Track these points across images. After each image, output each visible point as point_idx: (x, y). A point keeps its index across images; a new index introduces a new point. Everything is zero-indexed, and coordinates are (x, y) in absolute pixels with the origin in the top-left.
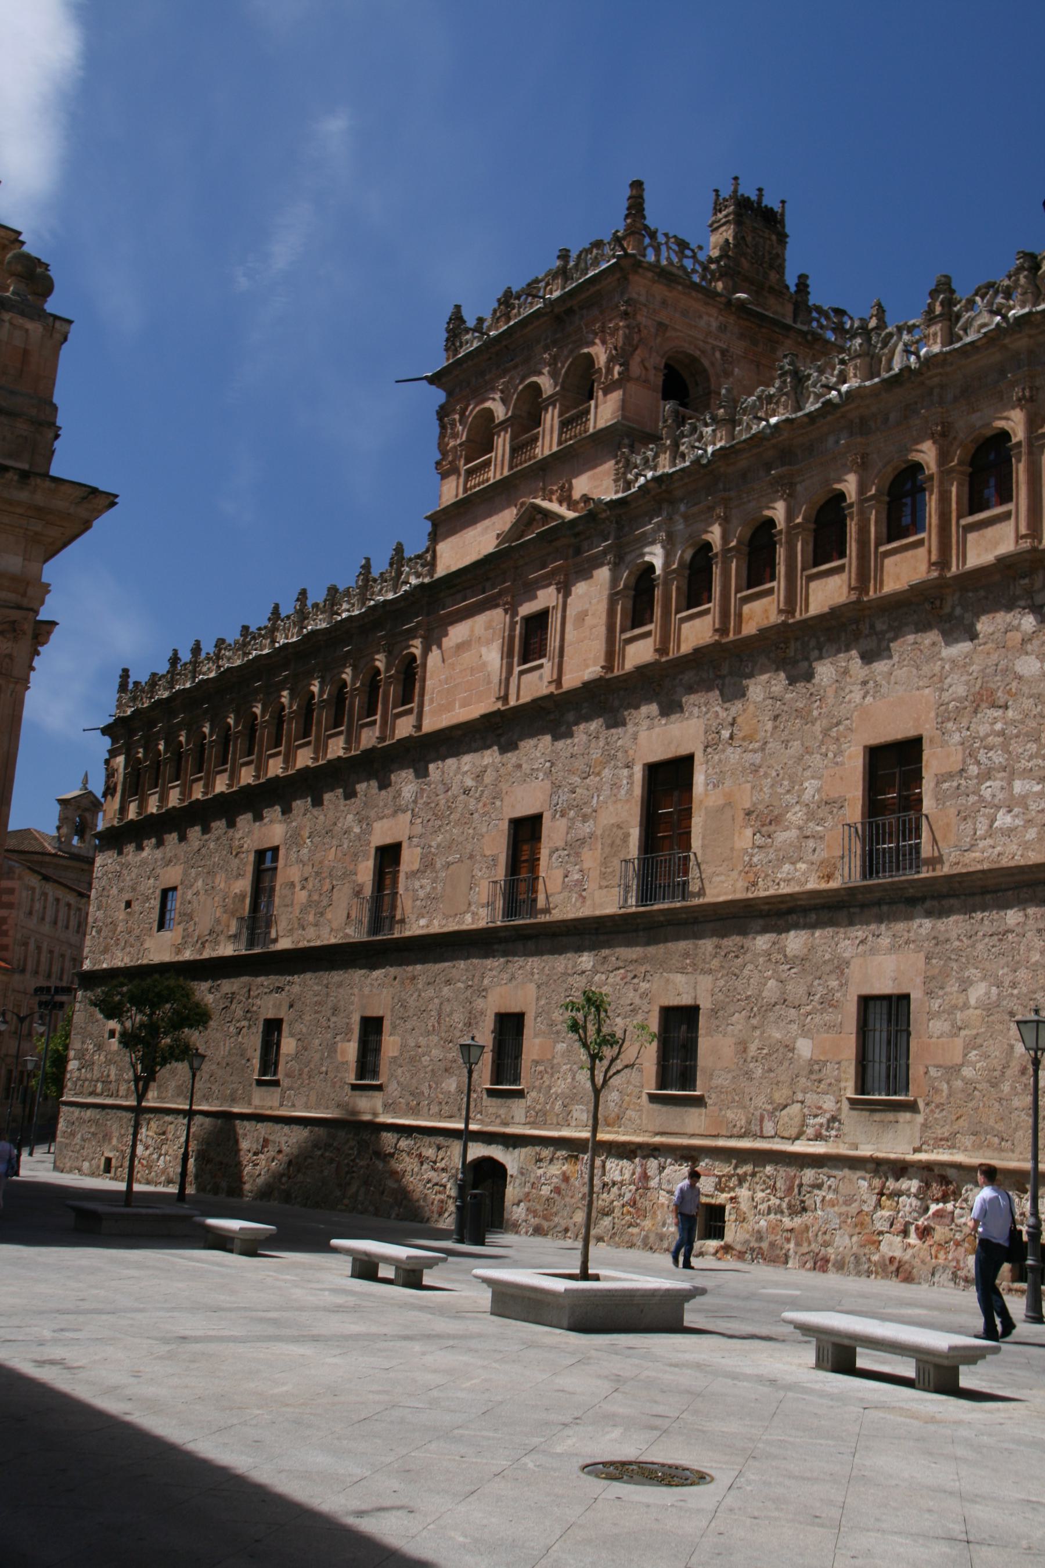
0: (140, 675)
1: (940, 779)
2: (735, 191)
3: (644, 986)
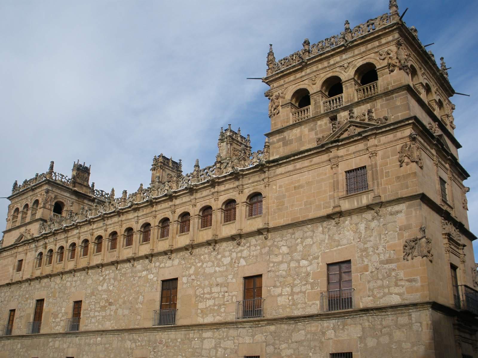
1: (85, 310)
2: (78, 163)
3: (29, 352)
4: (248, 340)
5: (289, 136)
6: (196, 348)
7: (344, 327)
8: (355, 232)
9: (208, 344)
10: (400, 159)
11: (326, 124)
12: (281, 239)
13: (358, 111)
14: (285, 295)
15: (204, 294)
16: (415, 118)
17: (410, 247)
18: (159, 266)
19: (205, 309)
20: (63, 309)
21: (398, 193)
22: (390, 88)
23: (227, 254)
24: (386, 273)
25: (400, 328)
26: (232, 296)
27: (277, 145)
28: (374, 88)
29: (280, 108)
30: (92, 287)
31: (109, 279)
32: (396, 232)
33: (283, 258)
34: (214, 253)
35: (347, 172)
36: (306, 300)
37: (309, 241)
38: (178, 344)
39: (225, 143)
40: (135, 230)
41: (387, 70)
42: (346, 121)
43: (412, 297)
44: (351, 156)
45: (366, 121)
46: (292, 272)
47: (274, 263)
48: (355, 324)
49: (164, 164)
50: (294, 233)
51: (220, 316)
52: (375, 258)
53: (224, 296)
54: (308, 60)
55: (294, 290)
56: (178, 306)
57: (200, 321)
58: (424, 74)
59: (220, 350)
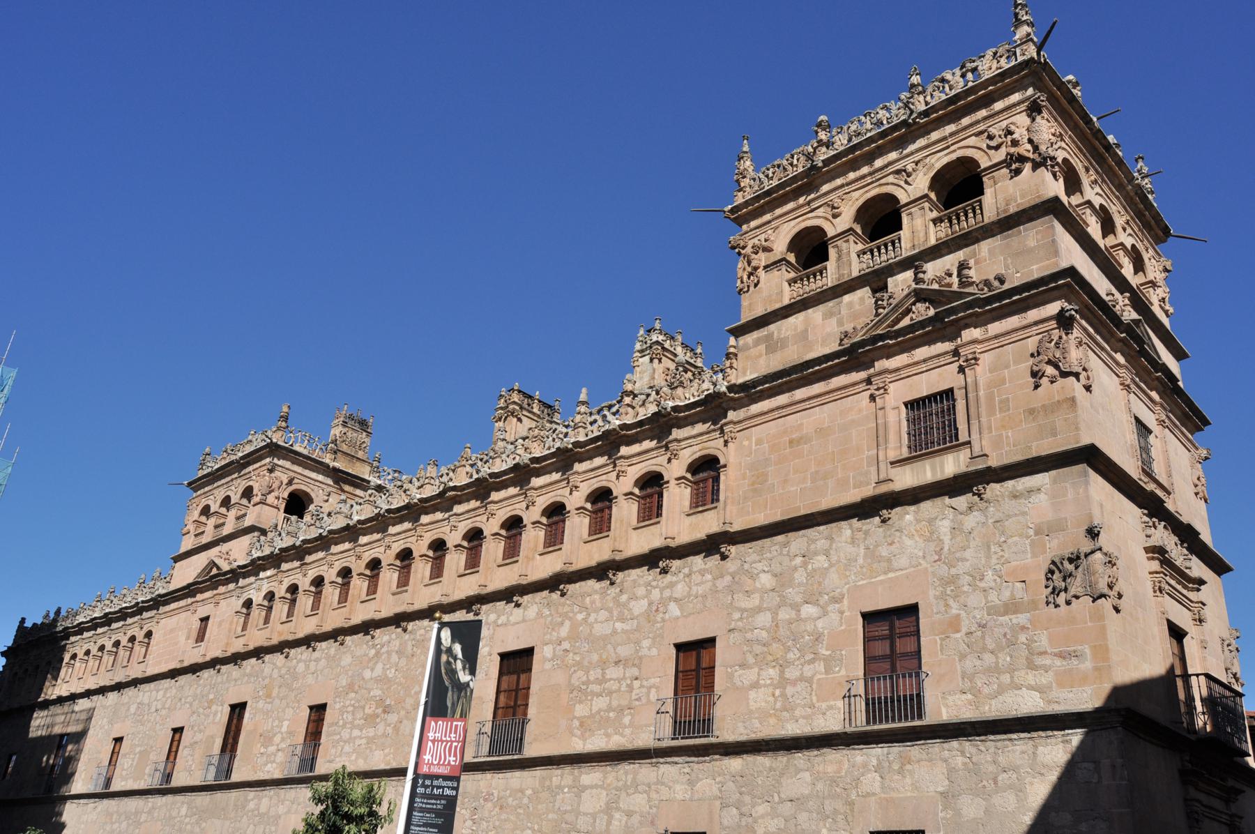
0: (28, 624)
1: (332, 724)
4: (681, 792)
5: (780, 331)
6: (566, 812)
7: (903, 765)
8: (928, 540)
9: (592, 802)
10: (1035, 368)
11: (862, 299)
12: (758, 558)
13: (933, 269)
14: (765, 686)
15: (587, 683)
16: (1072, 272)
17: (1062, 574)
18: (495, 622)
19: (588, 717)
20: (286, 723)
21: (1030, 448)
22: (1013, 209)
23: (641, 591)
24: (1005, 635)
25: (1042, 774)
26: (650, 688)
27: (754, 352)
28: (974, 212)
29: (761, 273)
30: (350, 673)
31: (389, 653)
32: (1028, 537)
33: (762, 598)
34: (613, 591)
35: (912, 405)
36: (814, 698)
37: (820, 561)
38: (525, 801)
39: (647, 358)
40: (449, 544)
41: (1005, 171)
42: (905, 292)
43: (1071, 695)
44: (920, 372)
45: (955, 287)
46: (783, 632)
47: (743, 610)
48: (930, 760)
49: (521, 408)
50: (786, 545)
51: (622, 735)
52: (975, 600)
53: (630, 687)
54: (826, 162)
55: (787, 675)
56: (532, 711)
57: (579, 746)
58: (1095, 182)
59: (617, 815)
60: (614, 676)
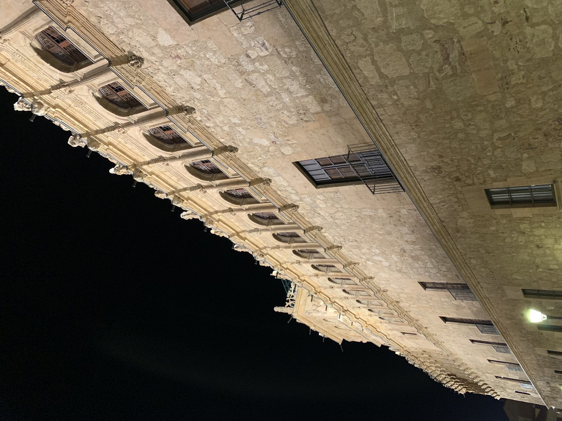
15: (286, 107)
53: (260, 59)
60: (264, 83)
